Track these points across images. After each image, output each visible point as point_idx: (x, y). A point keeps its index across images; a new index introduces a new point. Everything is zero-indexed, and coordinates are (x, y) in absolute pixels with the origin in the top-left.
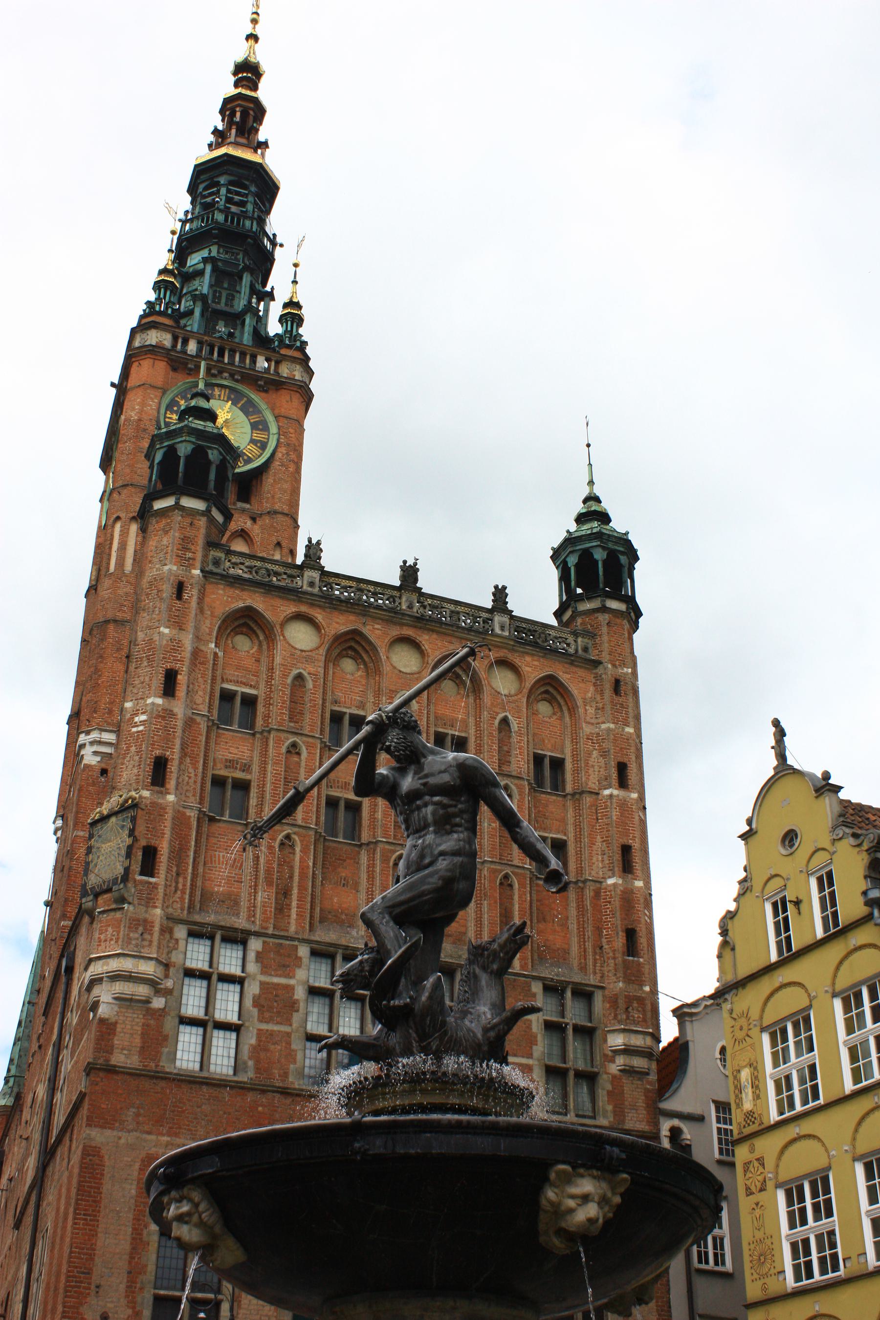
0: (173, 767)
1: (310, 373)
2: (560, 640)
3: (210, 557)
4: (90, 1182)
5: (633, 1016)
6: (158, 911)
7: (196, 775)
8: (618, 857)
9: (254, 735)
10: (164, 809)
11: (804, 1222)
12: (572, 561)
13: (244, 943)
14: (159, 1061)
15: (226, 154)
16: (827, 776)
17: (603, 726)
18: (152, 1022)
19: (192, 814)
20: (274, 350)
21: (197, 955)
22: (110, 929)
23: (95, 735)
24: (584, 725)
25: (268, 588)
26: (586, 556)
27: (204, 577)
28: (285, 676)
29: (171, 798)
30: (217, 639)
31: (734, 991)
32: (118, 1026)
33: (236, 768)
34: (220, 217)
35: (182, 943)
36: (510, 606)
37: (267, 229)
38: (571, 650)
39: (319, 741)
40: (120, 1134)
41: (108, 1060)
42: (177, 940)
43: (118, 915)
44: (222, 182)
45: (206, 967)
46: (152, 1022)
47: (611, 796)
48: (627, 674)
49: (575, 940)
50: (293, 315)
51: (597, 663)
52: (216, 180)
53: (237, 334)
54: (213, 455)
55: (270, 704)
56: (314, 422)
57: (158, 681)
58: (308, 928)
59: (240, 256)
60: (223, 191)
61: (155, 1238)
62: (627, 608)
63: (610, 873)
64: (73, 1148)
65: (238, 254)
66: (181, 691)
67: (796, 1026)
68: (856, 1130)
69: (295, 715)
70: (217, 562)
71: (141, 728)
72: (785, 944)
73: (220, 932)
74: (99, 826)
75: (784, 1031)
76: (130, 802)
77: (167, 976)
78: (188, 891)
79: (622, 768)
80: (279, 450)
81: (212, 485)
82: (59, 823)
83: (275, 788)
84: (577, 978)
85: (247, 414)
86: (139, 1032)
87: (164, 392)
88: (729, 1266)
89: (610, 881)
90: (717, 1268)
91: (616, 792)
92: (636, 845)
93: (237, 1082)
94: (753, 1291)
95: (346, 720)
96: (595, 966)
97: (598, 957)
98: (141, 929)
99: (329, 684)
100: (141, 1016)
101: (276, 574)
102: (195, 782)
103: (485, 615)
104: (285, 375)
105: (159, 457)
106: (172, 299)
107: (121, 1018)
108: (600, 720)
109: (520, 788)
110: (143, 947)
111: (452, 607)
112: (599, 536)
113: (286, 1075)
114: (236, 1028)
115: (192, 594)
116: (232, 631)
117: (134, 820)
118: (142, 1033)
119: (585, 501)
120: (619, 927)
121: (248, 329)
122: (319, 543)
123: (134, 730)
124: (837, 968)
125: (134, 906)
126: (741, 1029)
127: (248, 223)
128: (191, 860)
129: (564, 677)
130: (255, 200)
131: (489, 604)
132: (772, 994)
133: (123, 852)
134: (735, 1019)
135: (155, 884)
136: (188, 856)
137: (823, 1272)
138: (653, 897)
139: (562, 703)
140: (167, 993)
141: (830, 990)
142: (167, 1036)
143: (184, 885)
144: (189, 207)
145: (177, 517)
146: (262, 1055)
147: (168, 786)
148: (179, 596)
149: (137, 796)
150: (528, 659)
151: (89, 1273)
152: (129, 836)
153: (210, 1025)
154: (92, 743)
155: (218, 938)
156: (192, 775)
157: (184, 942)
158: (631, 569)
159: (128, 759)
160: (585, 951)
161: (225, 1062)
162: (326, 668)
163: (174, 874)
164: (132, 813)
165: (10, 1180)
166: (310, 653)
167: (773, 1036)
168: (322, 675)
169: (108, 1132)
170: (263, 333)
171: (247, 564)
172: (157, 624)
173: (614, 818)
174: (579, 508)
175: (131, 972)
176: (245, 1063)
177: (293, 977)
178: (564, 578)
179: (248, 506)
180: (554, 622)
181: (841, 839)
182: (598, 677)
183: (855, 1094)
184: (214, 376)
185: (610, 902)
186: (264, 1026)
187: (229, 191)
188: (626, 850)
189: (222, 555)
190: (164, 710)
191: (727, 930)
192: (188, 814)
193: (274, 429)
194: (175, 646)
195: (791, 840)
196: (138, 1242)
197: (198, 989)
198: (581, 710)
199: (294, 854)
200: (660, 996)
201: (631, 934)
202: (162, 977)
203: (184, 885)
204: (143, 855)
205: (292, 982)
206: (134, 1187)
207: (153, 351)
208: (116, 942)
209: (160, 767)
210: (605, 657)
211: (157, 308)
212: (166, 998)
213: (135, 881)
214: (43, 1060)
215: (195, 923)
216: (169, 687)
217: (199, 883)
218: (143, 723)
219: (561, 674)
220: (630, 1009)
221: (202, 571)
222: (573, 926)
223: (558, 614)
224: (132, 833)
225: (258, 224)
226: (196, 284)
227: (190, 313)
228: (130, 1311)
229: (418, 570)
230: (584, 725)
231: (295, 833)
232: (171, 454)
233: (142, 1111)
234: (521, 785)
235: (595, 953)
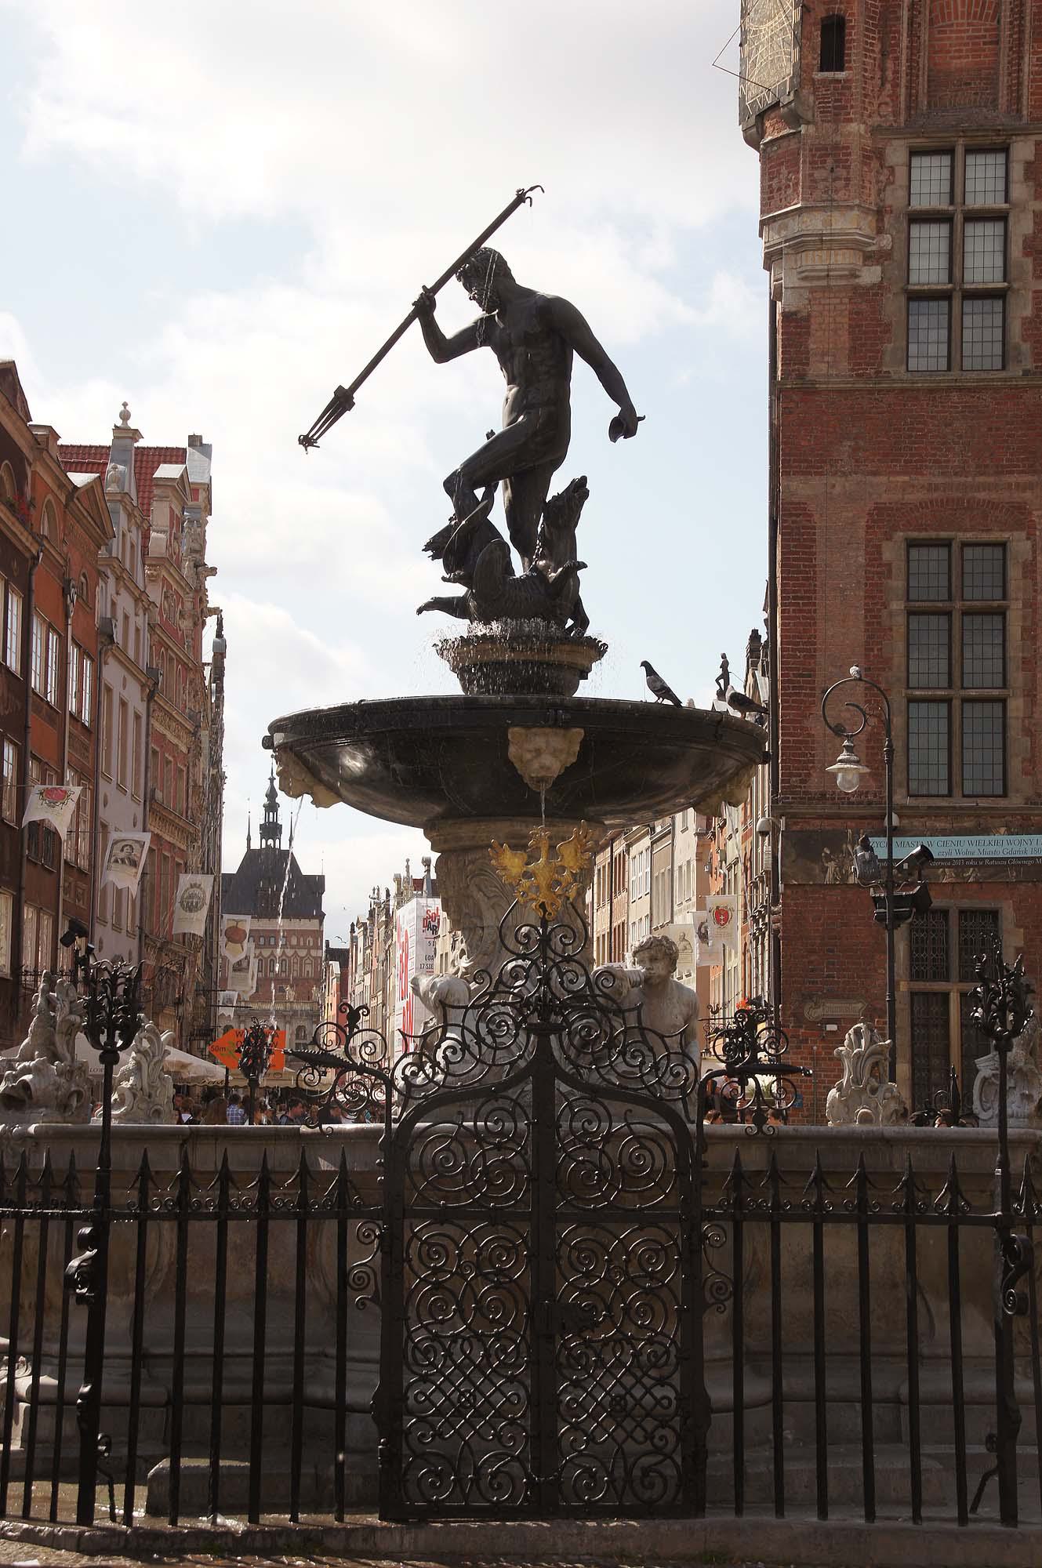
4: (797, 553)
13: (1005, 149)
14: (880, 365)
18: (864, 306)
21: (929, 182)
22: (784, 170)
35: (901, 173)
40: (832, 480)
41: (801, 376)
43: (793, 144)
45: (944, 206)
46: (864, 306)
61: (901, 620)
73: (961, 141)
77: (880, 231)
78: (903, 82)
86: (846, 326)
93: (1005, 380)
98: (830, 160)
100: (846, 300)
107: (815, 308)
110: (837, 191)
114: (1000, 295)
118: (850, 326)
128: (905, 25)
135: (847, 81)
136: (898, 19)
142: (890, 324)
151: (811, 673)
155: (960, 151)
157: (905, 169)
169: (815, 481)
175: (822, 235)
196: (876, 629)
202: (873, 234)
203: (896, 72)
206: (862, 552)
217: (923, 61)
233: (861, 443)
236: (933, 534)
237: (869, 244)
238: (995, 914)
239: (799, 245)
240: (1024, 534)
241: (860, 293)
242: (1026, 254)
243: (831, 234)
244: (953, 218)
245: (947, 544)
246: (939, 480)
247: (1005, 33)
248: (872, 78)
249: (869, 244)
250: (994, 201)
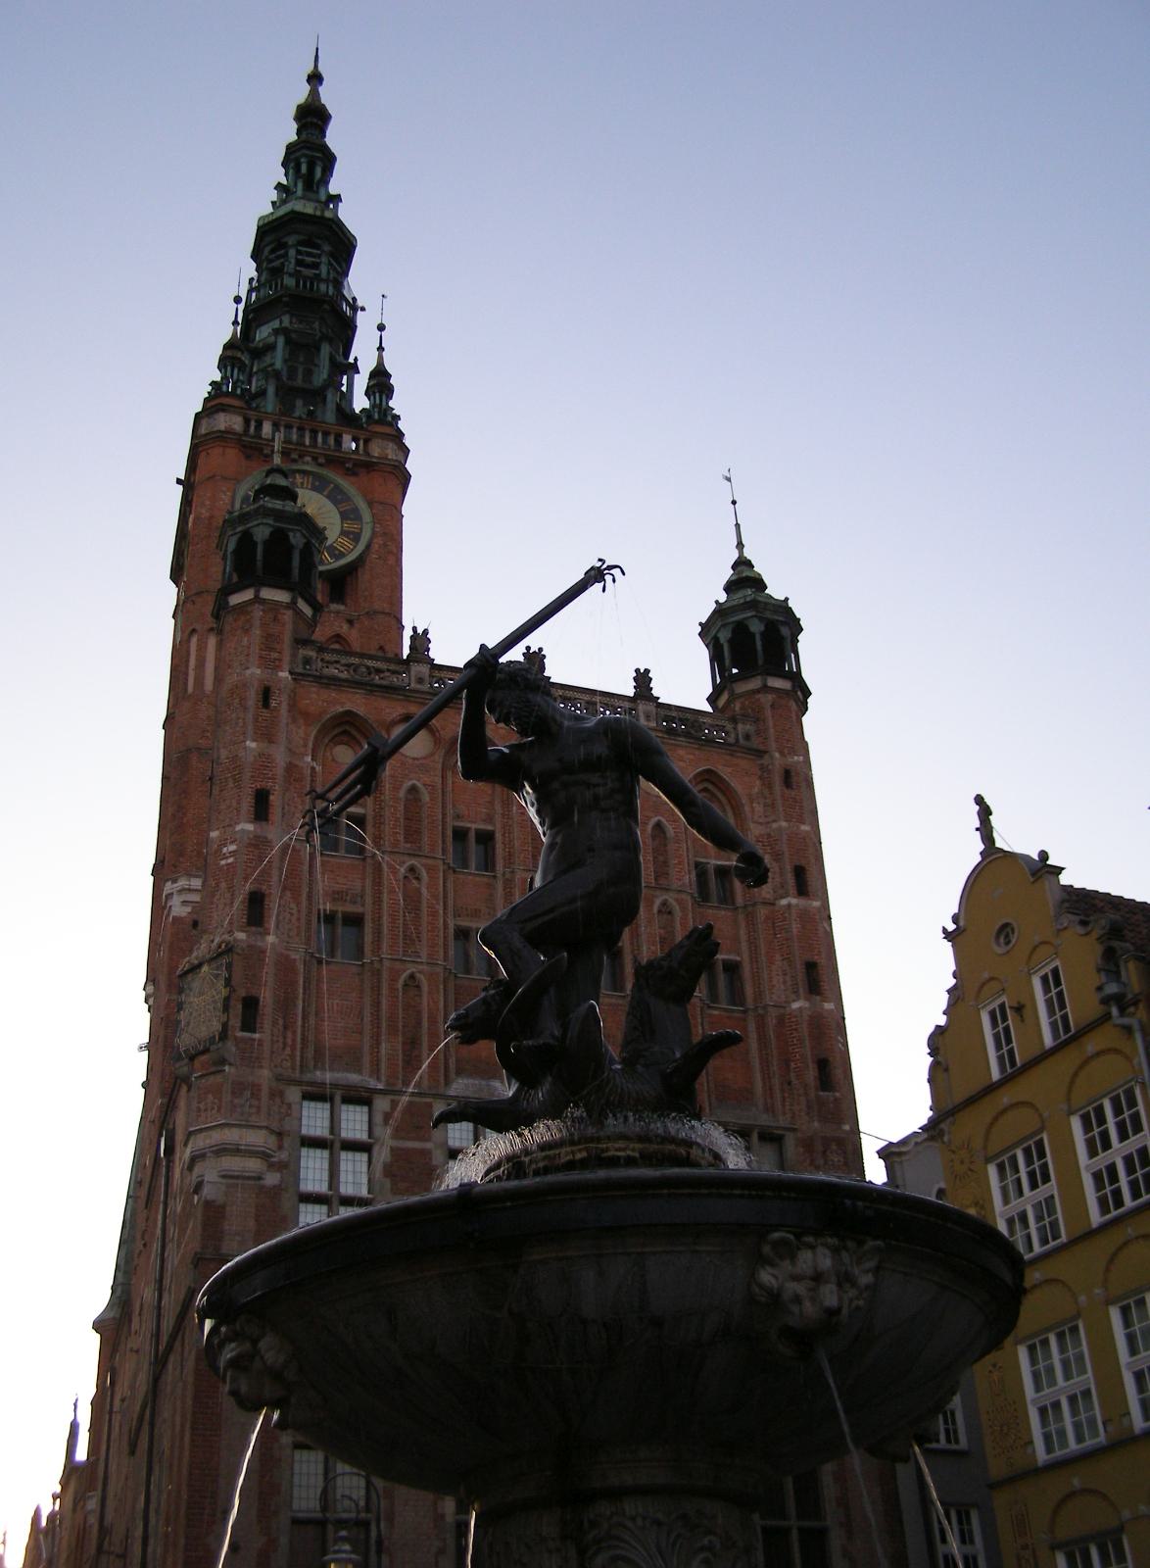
0: (273, 907)
1: (406, 451)
2: (717, 728)
3: (300, 656)
5: (833, 1161)
6: (266, 1073)
7: (299, 911)
8: (801, 975)
9: (364, 859)
10: (264, 952)
11: (1052, 1382)
12: (724, 636)
15: (293, 212)
16: (1044, 855)
17: (775, 825)
19: (298, 957)
20: (362, 428)
21: (314, 1119)
22: (210, 1096)
23: (182, 883)
24: (752, 826)
25: (371, 688)
26: (740, 629)
27: (294, 679)
28: (396, 788)
29: (271, 939)
30: (313, 750)
31: (951, 1119)
32: (228, 1208)
33: (346, 900)
34: (289, 282)
36: (655, 693)
37: (345, 293)
38: (731, 740)
39: (441, 862)
42: (289, 1106)
43: (219, 1078)
44: (290, 243)
47: (789, 905)
48: (799, 762)
49: (758, 1076)
50: (381, 384)
51: (760, 753)
52: (284, 240)
53: (319, 413)
54: (297, 539)
55: (380, 823)
56: (413, 507)
57: (247, 803)
58: (442, 1081)
59: (316, 325)
60: (292, 252)
62: (794, 686)
63: (793, 996)
64: (186, 1355)
65: (314, 323)
66: (276, 813)
67: (1027, 1152)
68: (1107, 1270)
69: (412, 833)
70: (307, 661)
71: (231, 860)
72: (1007, 1058)
74: (190, 977)
75: (1014, 1160)
76: (223, 947)
77: (280, 1147)
78: (299, 1046)
79: (800, 873)
80: (375, 541)
81: (296, 572)
82: (151, 988)
83: (393, 921)
84: (764, 1120)
85: (335, 502)
87: (238, 481)
88: (964, 1442)
89: (795, 1006)
90: (948, 1447)
91: (794, 901)
92: (822, 961)
94: (997, 1468)
95: (472, 836)
96: (784, 1106)
97: (786, 1095)
99: (449, 796)
100: (254, 1196)
101: (378, 671)
102: (299, 919)
103: (627, 705)
104: (376, 455)
105: (232, 546)
106: (241, 378)
108: (770, 819)
109: (680, 902)
110: (250, 1115)
111: (587, 698)
112: (752, 605)
115: (281, 702)
116: (330, 741)
117: (229, 966)
119: (734, 567)
120: (809, 1056)
121: (331, 406)
122: (426, 632)
123: (223, 862)
124: (1072, 1082)
125: (237, 1068)
126: (962, 1162)
127: (323, 287)
129: (724, 772)
130: (329, 261)
131: (630, 692)
132: (996, 1119)
133: (220, 1005)
134: (954, 1152)
137: (1080, 1439)
138: (846, 1021)
139: (723, 799)
140: (281, 1166)
141: (1065, 1107)
143: (294, 1040)
144: (254, 274)
145: (257, 612)
147: (266, 925)
148: (266, 703)
149: (231, 939)
150: (681, 752)
152: (225, 987)
153: (335, 1202)
154: (181, 891)
155: (338, 1099)
156: (294, 911)
158: (795, 642)
159: (217, 897)
160: (771, 1089)
162: (443, 777)
163: (281, 1028)
164: (224, 961)
165: (123, 1400)
166: (424, 761)
167: (1001, 1168)
168: (439, 786)
170: (348, 411)
171: (343, 662)
172: (242, 738)
173: (795, 931)
174: (727, 573)
177: (428, 1140)
178: (716, 657)
179: (342, 607)
180: (708, 708)
181: (1066, 928)
182: (762, 768)
183: (1104, 1227)
184: (294, 461)
185: (796, 1030)
187: (299, 252)
188: (811, 967)
189: (313, 654)
190: (256, 837)
191: (938, 1049)
192: (293, 957)
193: (367, 516)
194: (264, 762)
195: (1007, 936)
197: (318, 1161)
198: (747, 809)
199: (420, 996)
200: (862, 1135)
201: (823, 1065)
204: (243, 1008)
205: (429, 1145)
207: (223, 437)
208: (219, 1110)
209: (256, 904)
210: (773, 745)
211: (224, 388)
212: (281, 1172)
213: (236, 1038)
214: (149, 1257)
216: (261, 806)
218: (233, 853)
219: (720, 767)
220: (828, 1153)
221: (291, 673)
222: (756, 1064)
223: (711, 700)
224: (228, 982)
225: (334, 287)
226: (268, 359)
227: (262, 393)
229: (544, 656)
230: (752, 826)
231: (420, 972)
232: (246, 541)
234: (682, 900)
235: (783, 1091)
237: (272, 1156)
239: (222, 1151)
241: (262, 1190)
243: (246, 1145)
244: (332, 1145)
247: (367, 1028)
248: (278, 1041)
249: (272, 1156)
250: (362, 1135)
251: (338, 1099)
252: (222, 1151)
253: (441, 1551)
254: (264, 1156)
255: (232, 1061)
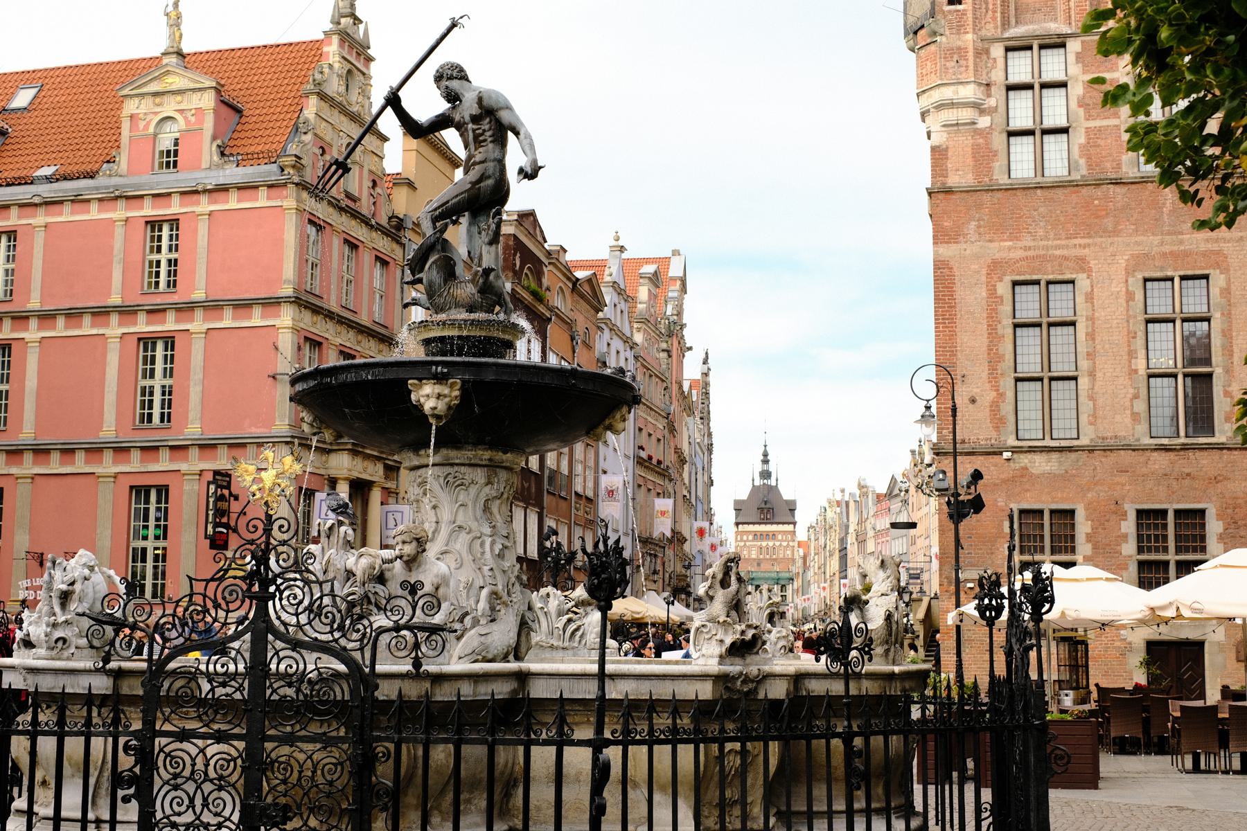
6: (970, 37)
13: (1063, 45)
18: (981, 141)
22: (929, 63)
43: (933, 47)
61: (1010, 330)
77: (989, 96)
98: (956, 57)
113: (1119, 166)
114: (1064, 131)
140: (991, 111)
146: (1092, 151)
153: (1038, 133)
155: (1035, 47)
161: (1059, 165)
169: (953, 246)
176: (1076, 162)
186: (1092, 124)
215: (1009, 39)
228: (994, 394)
236: (1028, 277)
238: (1071, 513)
239: (940, 107)
240: (1085, 275)
242: (1080, 106)
245: (1037, 282)
246: (1032, 244)
251: (1035, 47)
252: (940, 107)
253: (1136, 397)
254: (976, 106)
255: (942, 31)
